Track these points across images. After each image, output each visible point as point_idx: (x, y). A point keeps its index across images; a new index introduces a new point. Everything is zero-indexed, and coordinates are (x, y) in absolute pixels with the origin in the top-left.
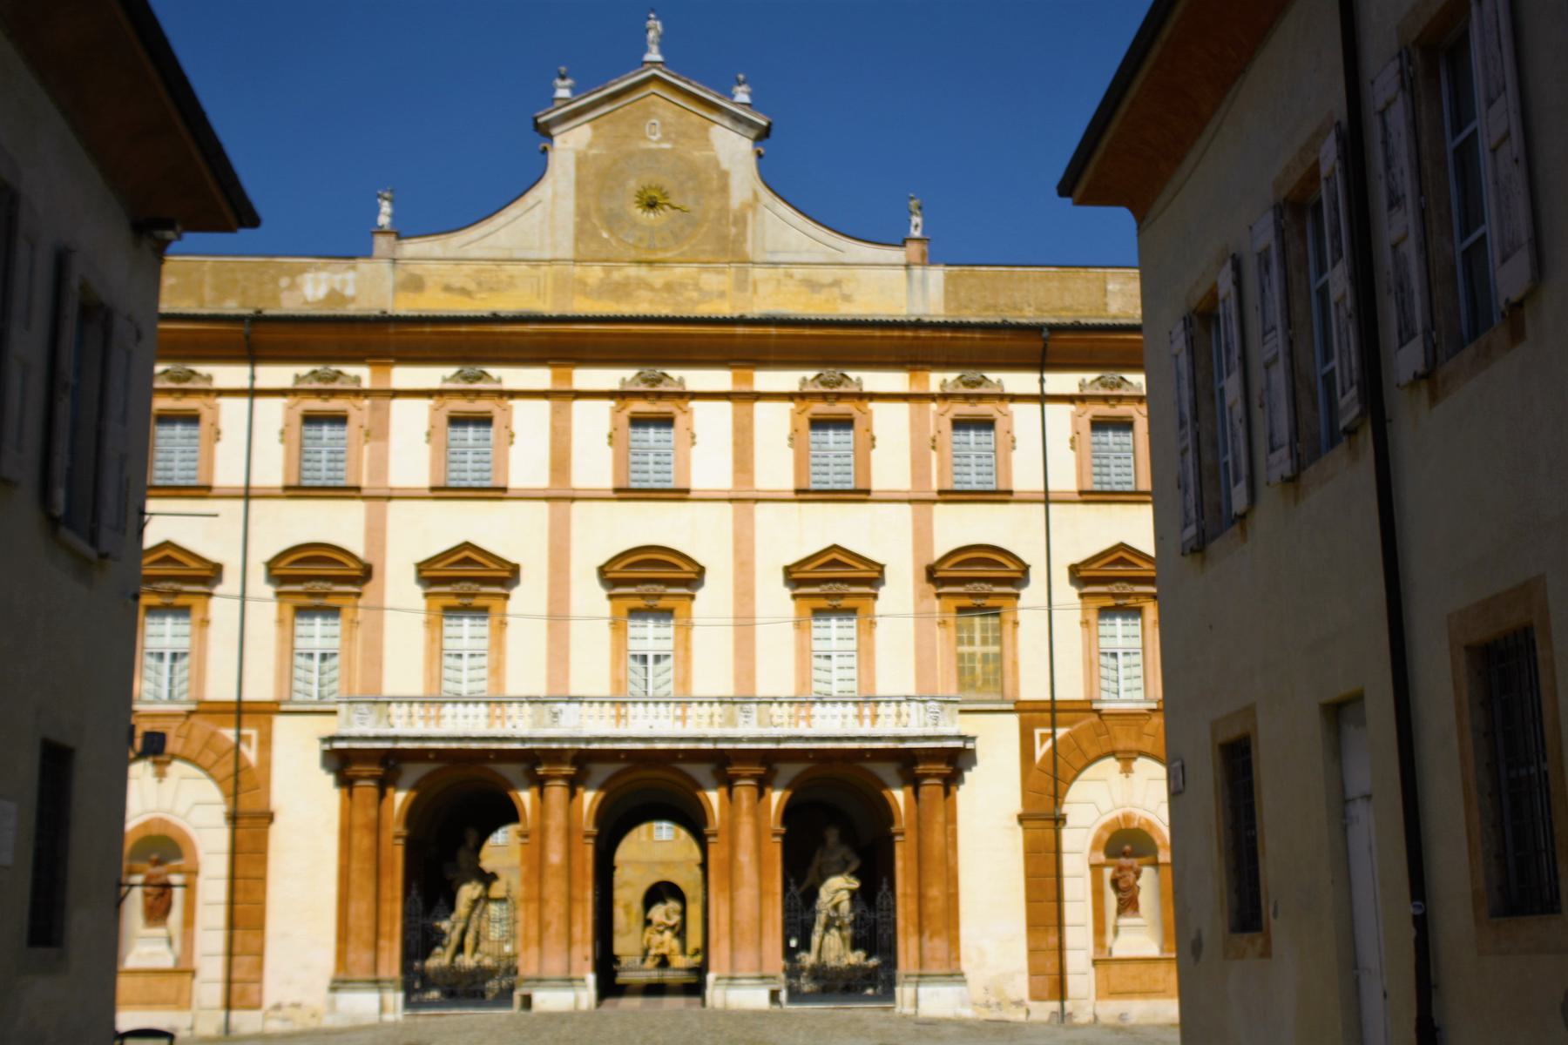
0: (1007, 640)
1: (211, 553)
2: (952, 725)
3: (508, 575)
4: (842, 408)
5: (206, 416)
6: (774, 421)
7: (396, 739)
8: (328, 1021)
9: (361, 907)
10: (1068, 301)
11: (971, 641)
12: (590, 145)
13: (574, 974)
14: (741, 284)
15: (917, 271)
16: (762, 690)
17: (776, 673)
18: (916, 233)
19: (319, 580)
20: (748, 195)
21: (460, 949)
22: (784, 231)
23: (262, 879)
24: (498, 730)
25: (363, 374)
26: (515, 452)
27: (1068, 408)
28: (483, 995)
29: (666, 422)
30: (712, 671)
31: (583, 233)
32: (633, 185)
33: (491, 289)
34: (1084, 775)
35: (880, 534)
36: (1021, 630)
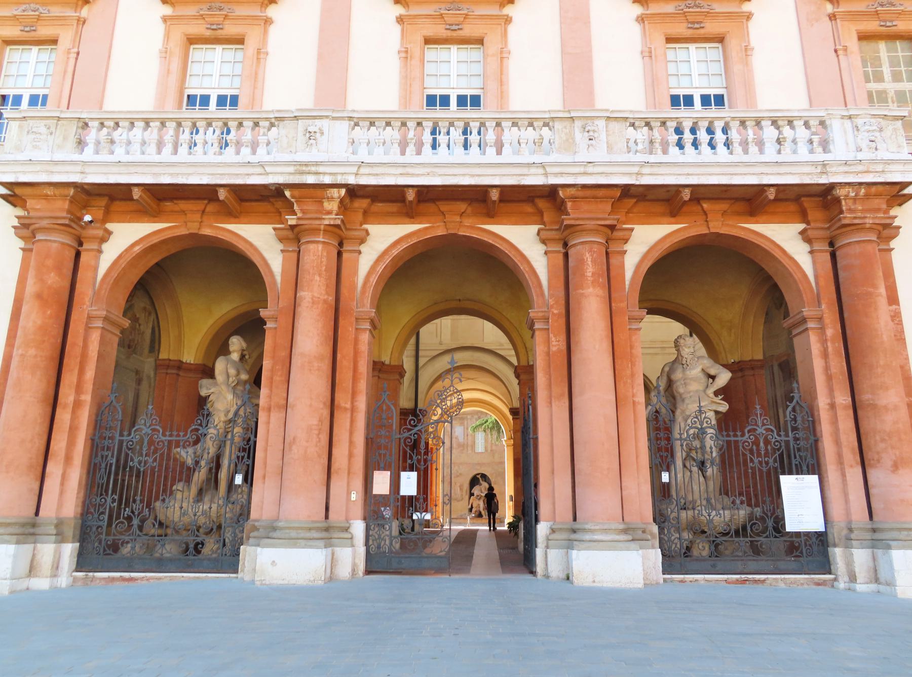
11: (879, 78)
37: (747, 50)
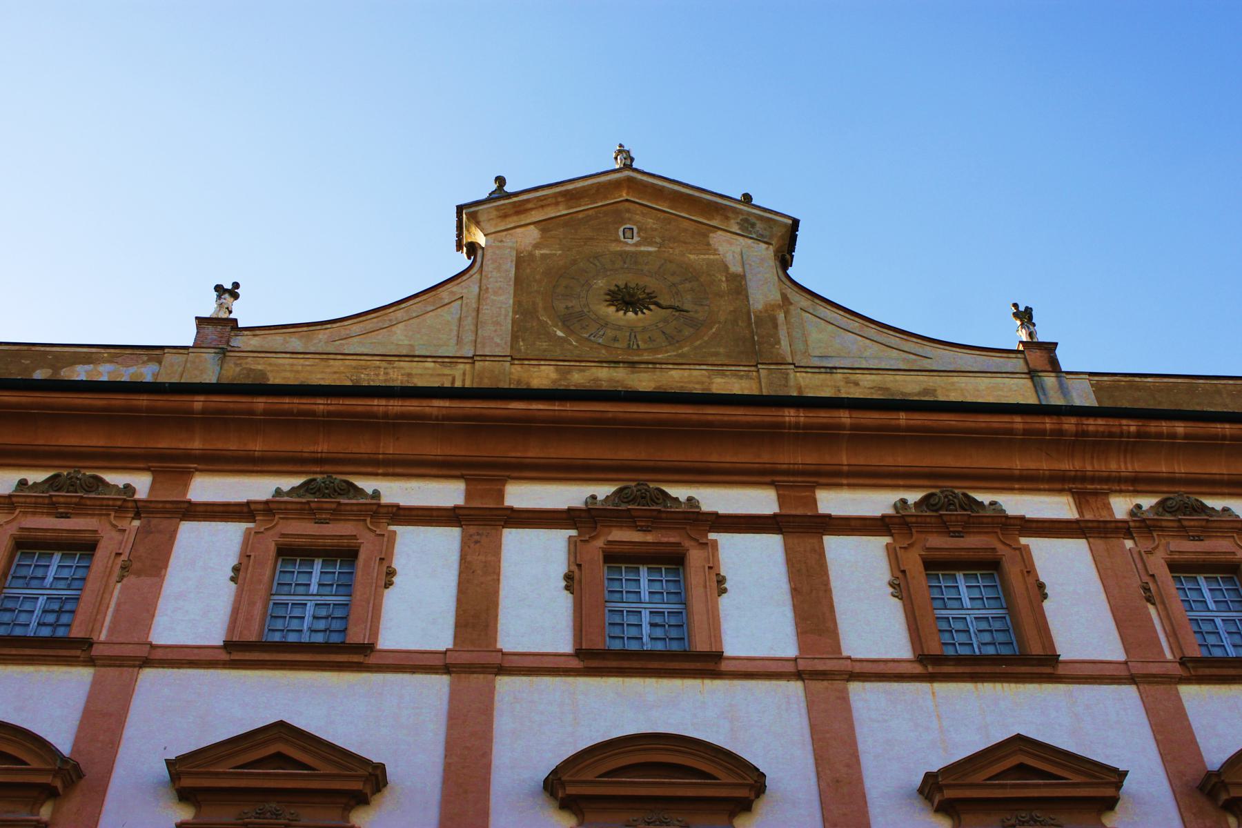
4: (973, 541)
12: (537, 246)
20: (775, 296)
25: (142, 484)
26: (392, 601)
32: (601, 283)
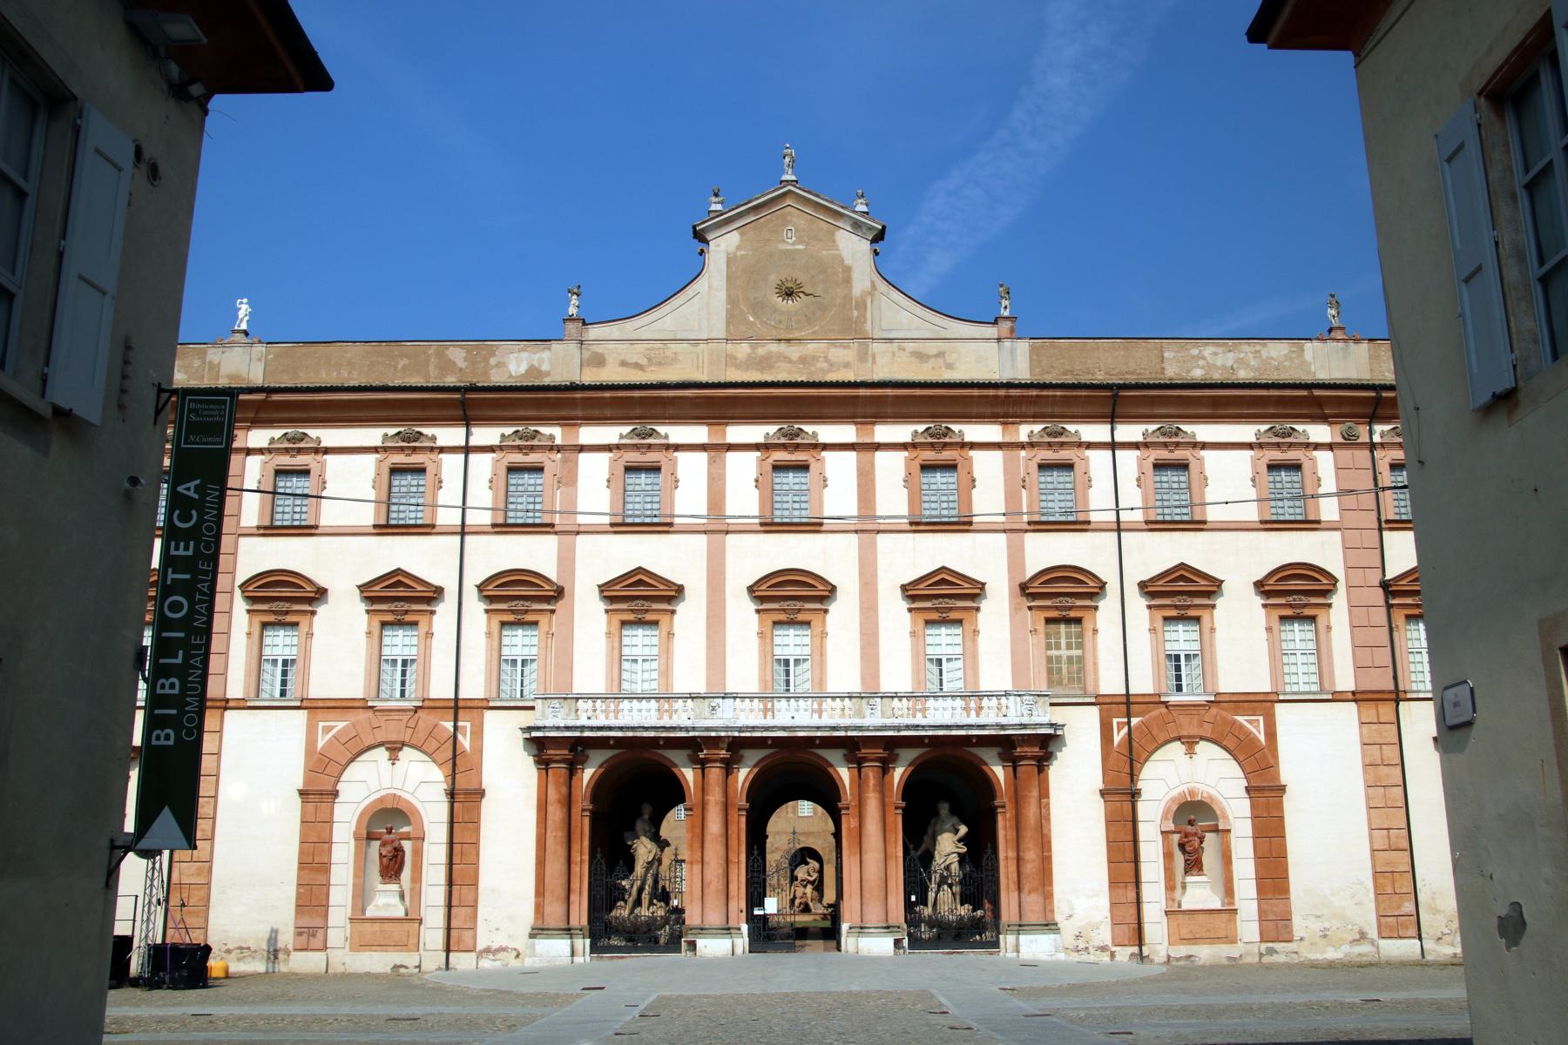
0: (1088, 645)
1: (435, 580)
2: (1043, 716)
3: (675, 593)
4: (947, 455)
5: (431, 469)
6: (892, 466)
7: (583, 728)
8: (529, 962)
9: (555, 867)
10: (1132, 366)
11: (1058, 647)
12: (738, 248)
13: (731, 924)
14: (863, 356)
15: (1007, 344)
16: (886, 686)
17: (897, 674)
18: (1006, 313)
19: (521, 598)
20: (868, 285)
21: (638, 902)
22: (896, 314)
23: (476, 844)
24: (666, 721)
25: (556, 433)
27: (1136, 453)
28: (657, 941)
29: (803, 467)
30: (843, 674)
31: (731, 318)
32: (774, 279)
33: (660, 364)
34: (1156, 756)
35: (979, 557)
36: (1100, 636)
37: (976, 632)
